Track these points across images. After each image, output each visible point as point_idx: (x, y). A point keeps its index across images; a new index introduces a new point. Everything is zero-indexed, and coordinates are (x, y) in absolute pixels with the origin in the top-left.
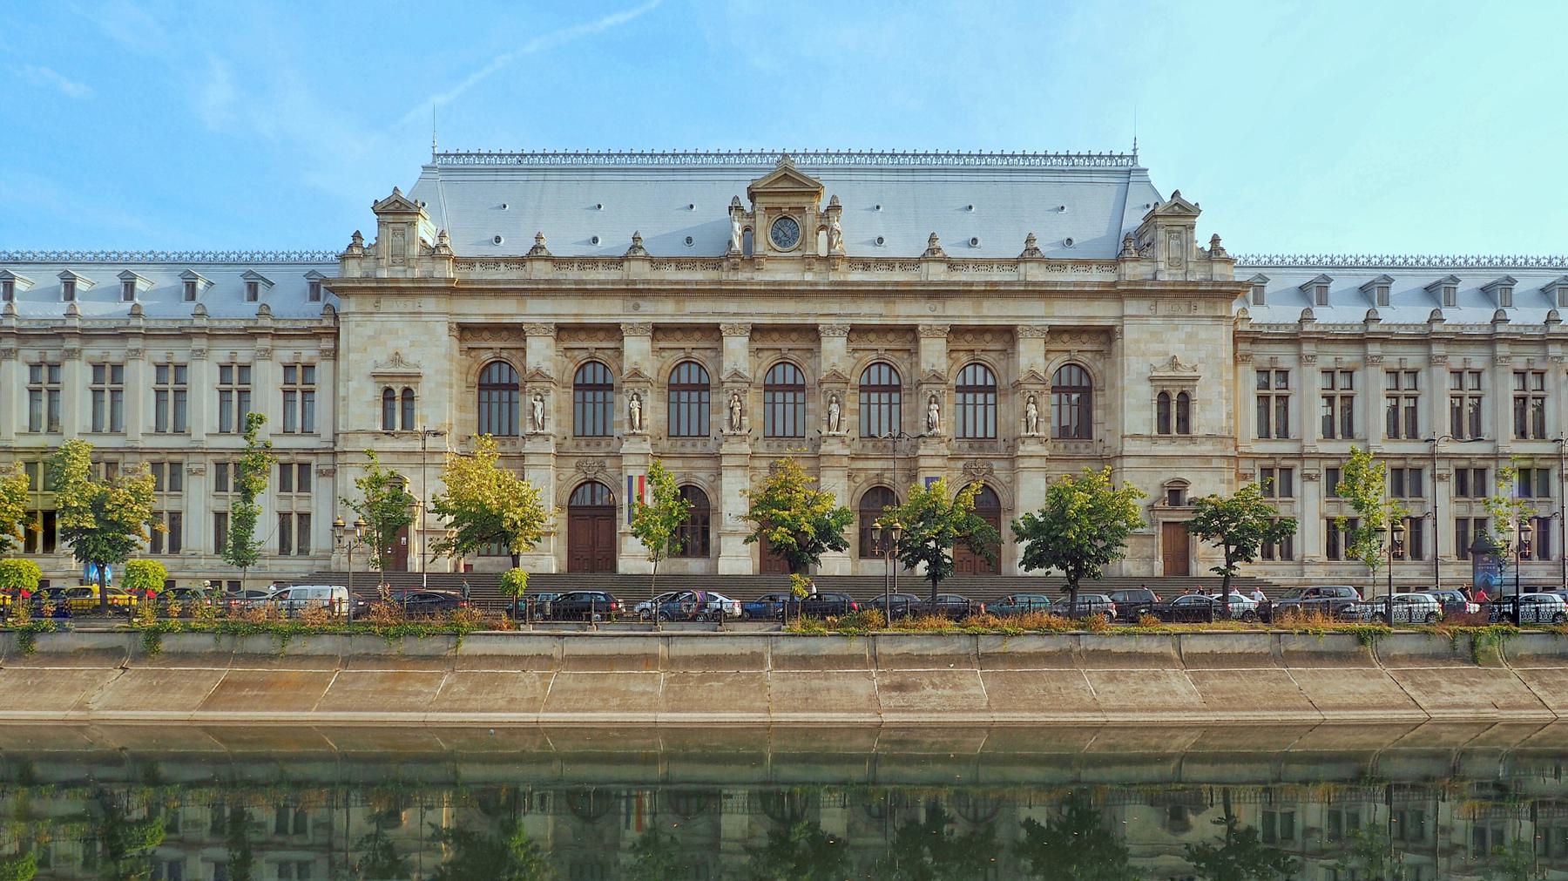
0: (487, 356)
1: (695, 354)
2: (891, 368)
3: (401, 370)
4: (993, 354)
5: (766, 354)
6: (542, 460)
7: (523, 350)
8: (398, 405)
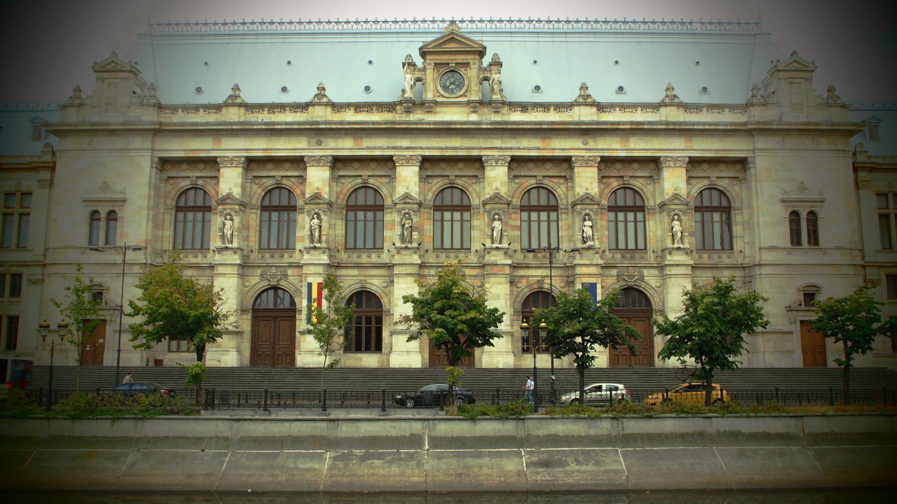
0: (185, 184)
1: (372, 181)
2: (549, 191)
3: (109, 195)
4: (641, 181)
5: (435, 180)
6: (229, 270)
7: (217, 178)
8: (103, 224)
